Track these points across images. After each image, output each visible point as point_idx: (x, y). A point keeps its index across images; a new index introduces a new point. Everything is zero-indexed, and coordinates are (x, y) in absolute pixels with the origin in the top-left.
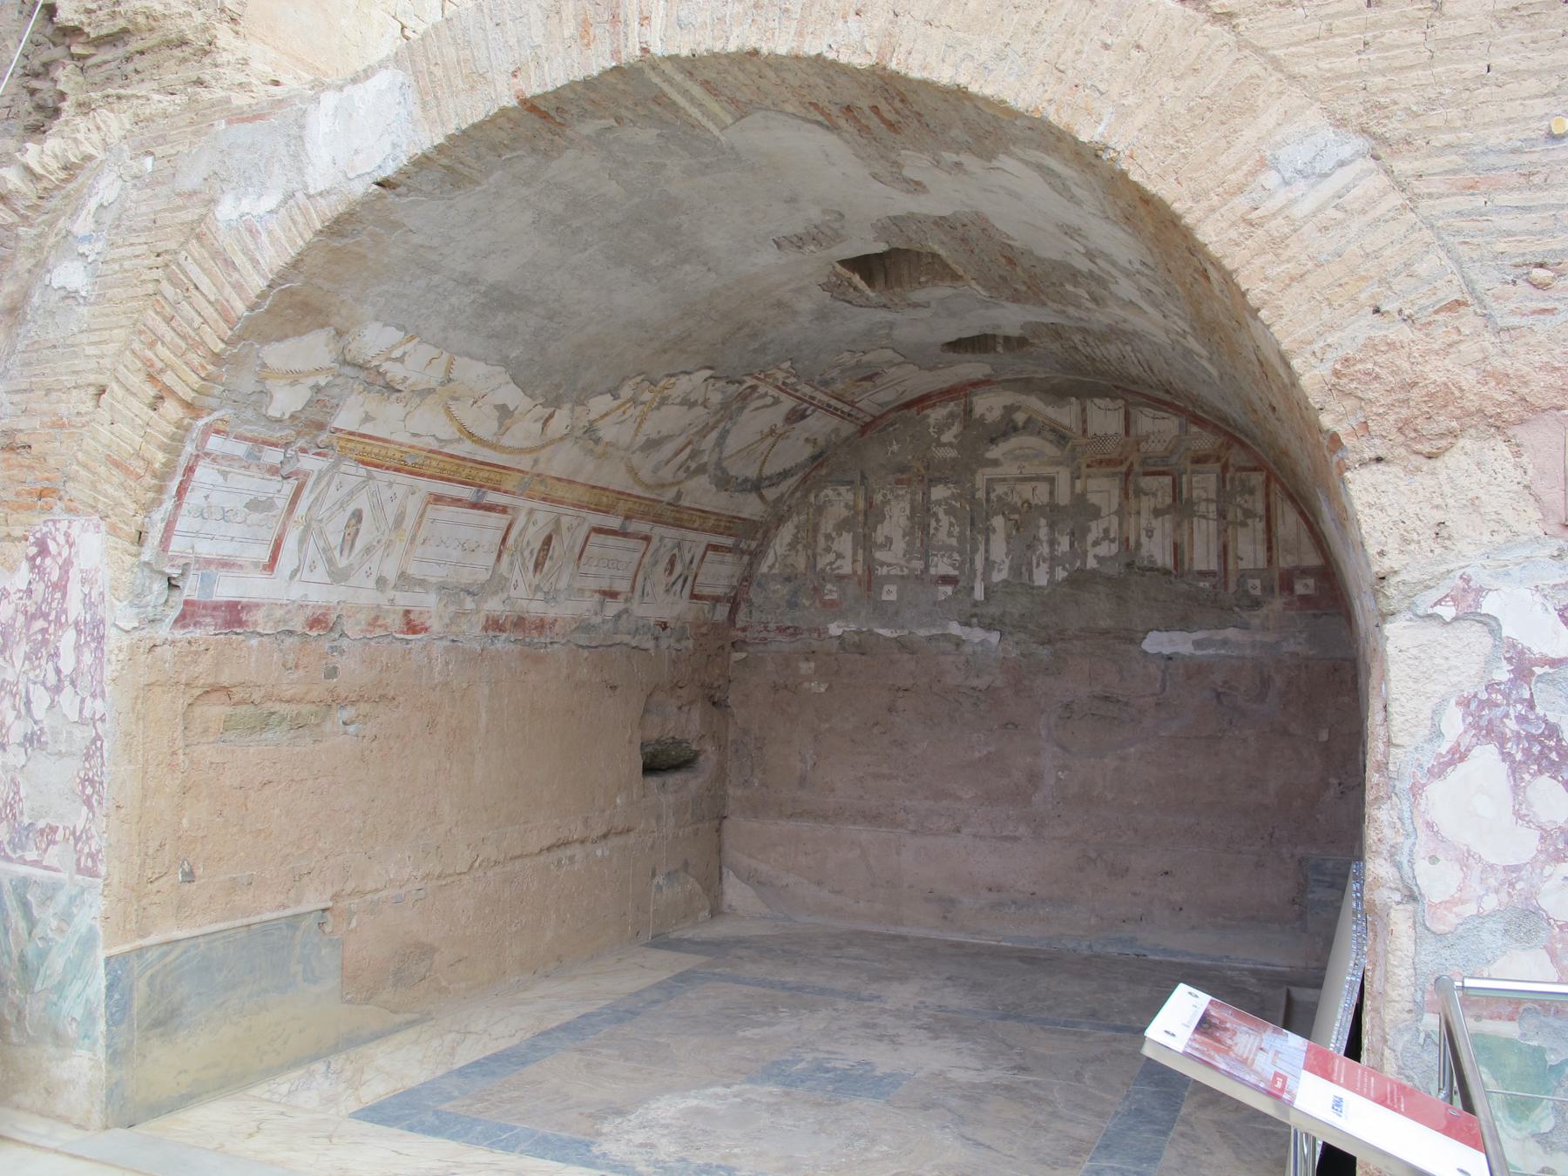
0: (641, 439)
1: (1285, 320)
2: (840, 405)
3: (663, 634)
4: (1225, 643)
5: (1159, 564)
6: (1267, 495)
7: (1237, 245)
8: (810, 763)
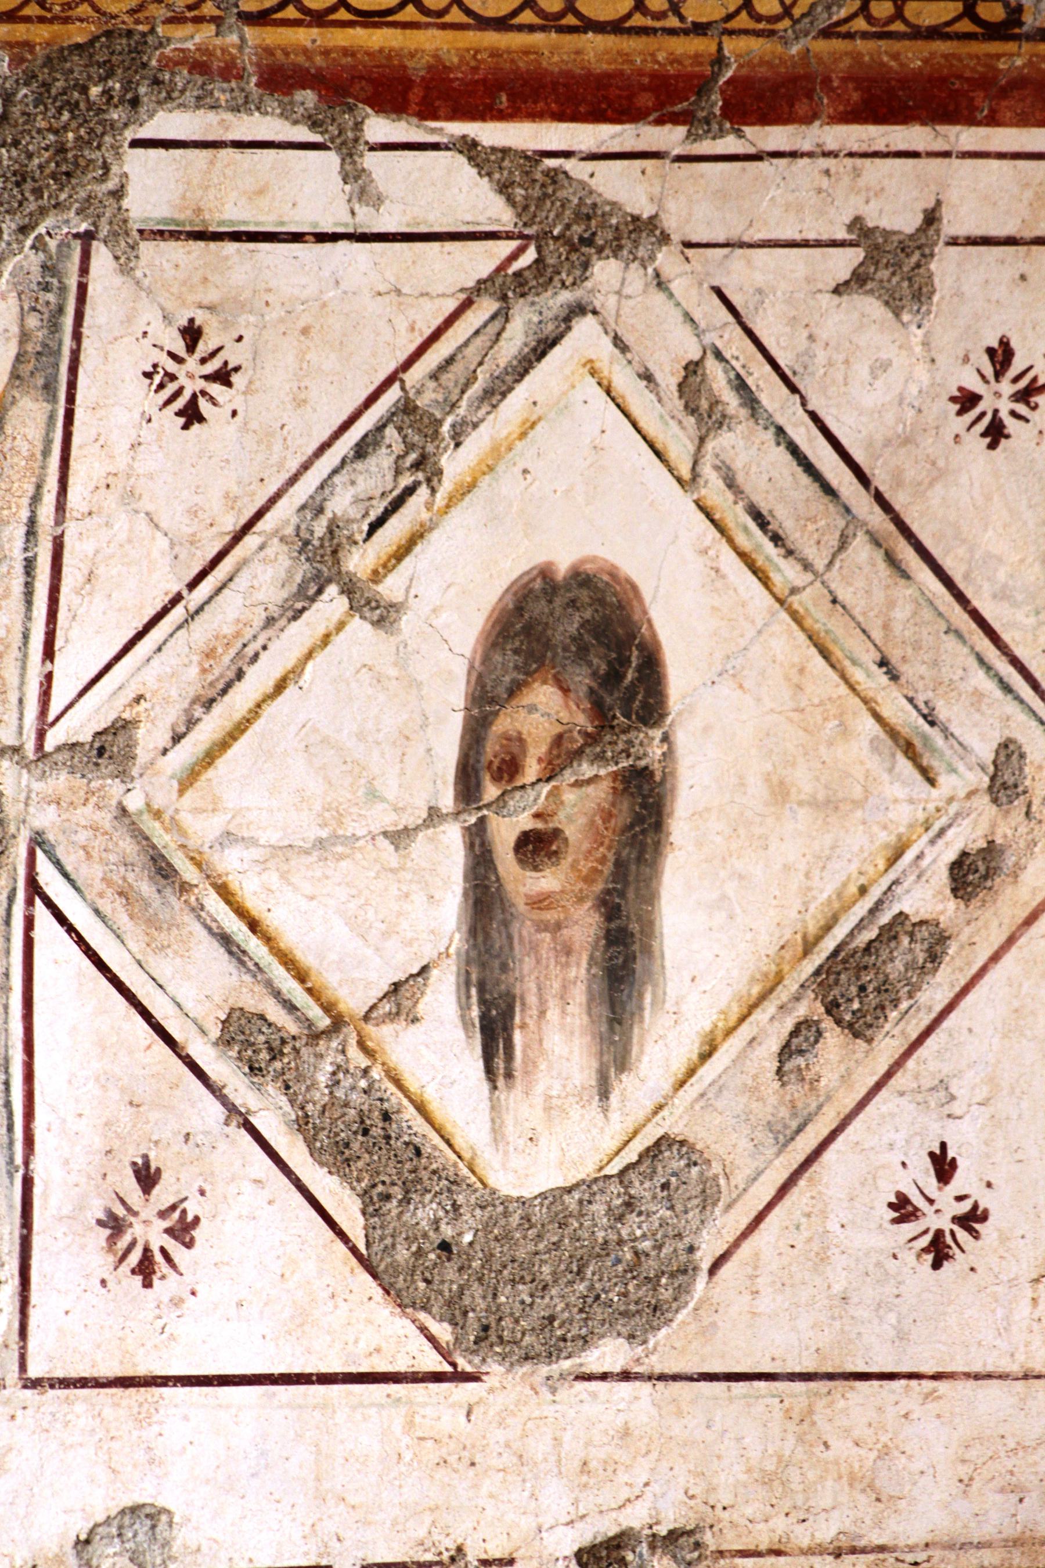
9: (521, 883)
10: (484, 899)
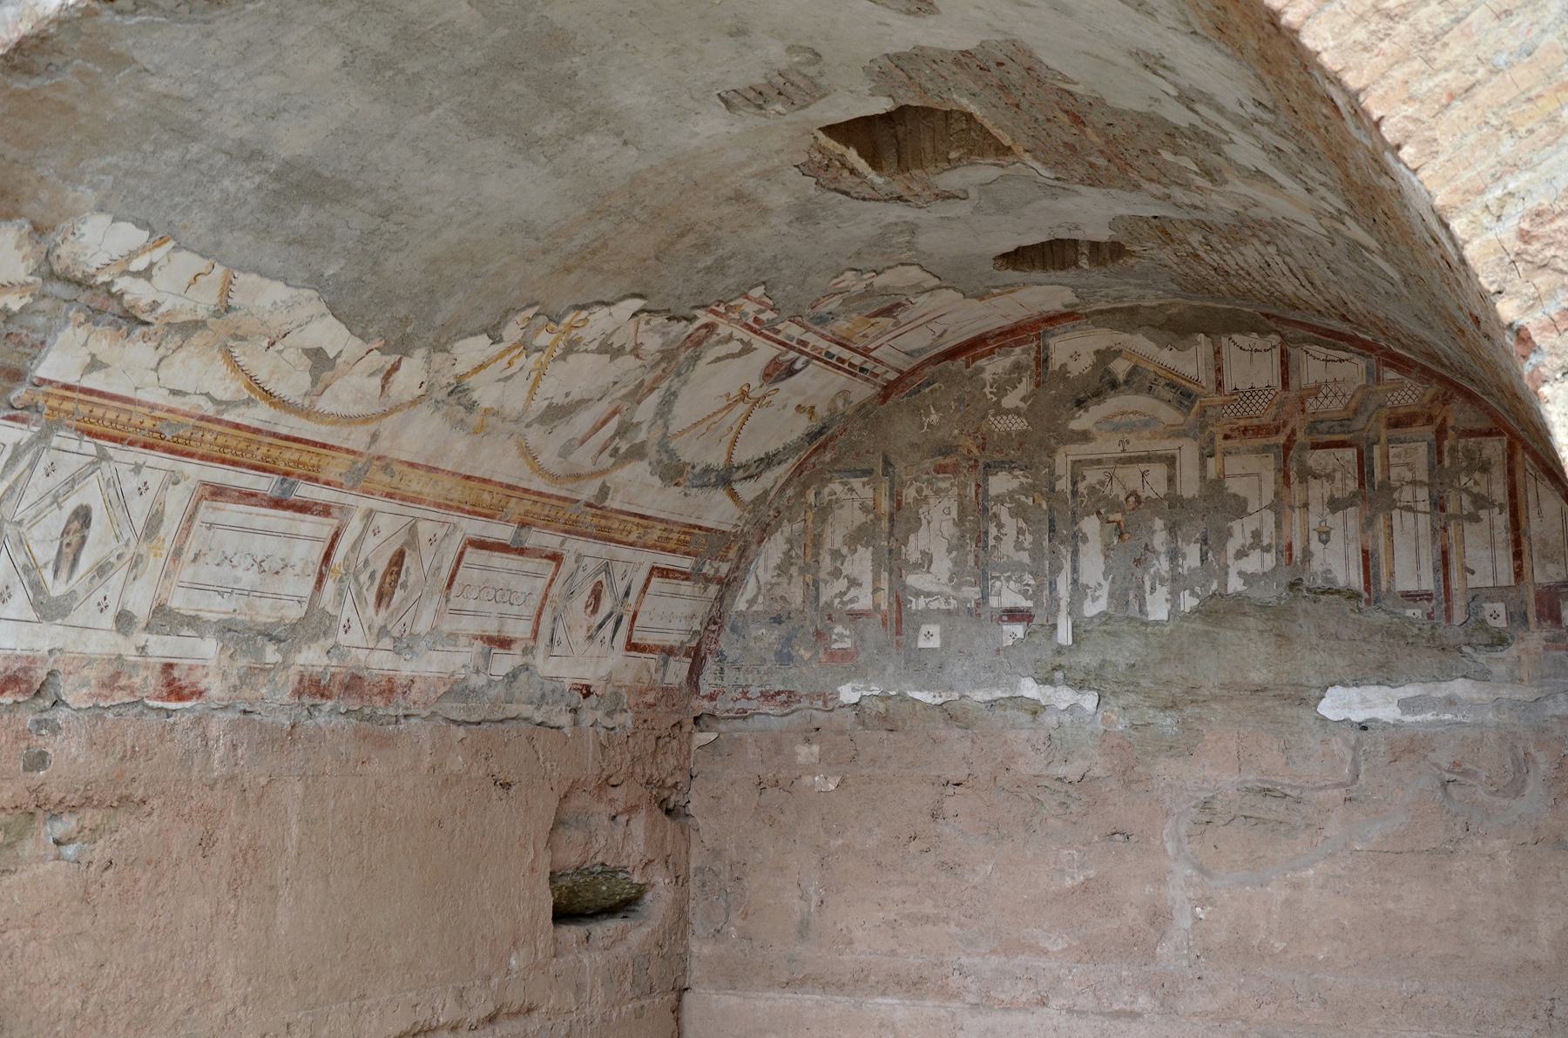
0: (539, 405)
1: (1442, 158)
2: (846, 354)
3: (585, 703)
4: (1451, 702)
5: (1341, 582)
6: (1511, 472)
7: (1366, 49)
8: (815, 900)
9: (65, 550)
10: (60, 552)
